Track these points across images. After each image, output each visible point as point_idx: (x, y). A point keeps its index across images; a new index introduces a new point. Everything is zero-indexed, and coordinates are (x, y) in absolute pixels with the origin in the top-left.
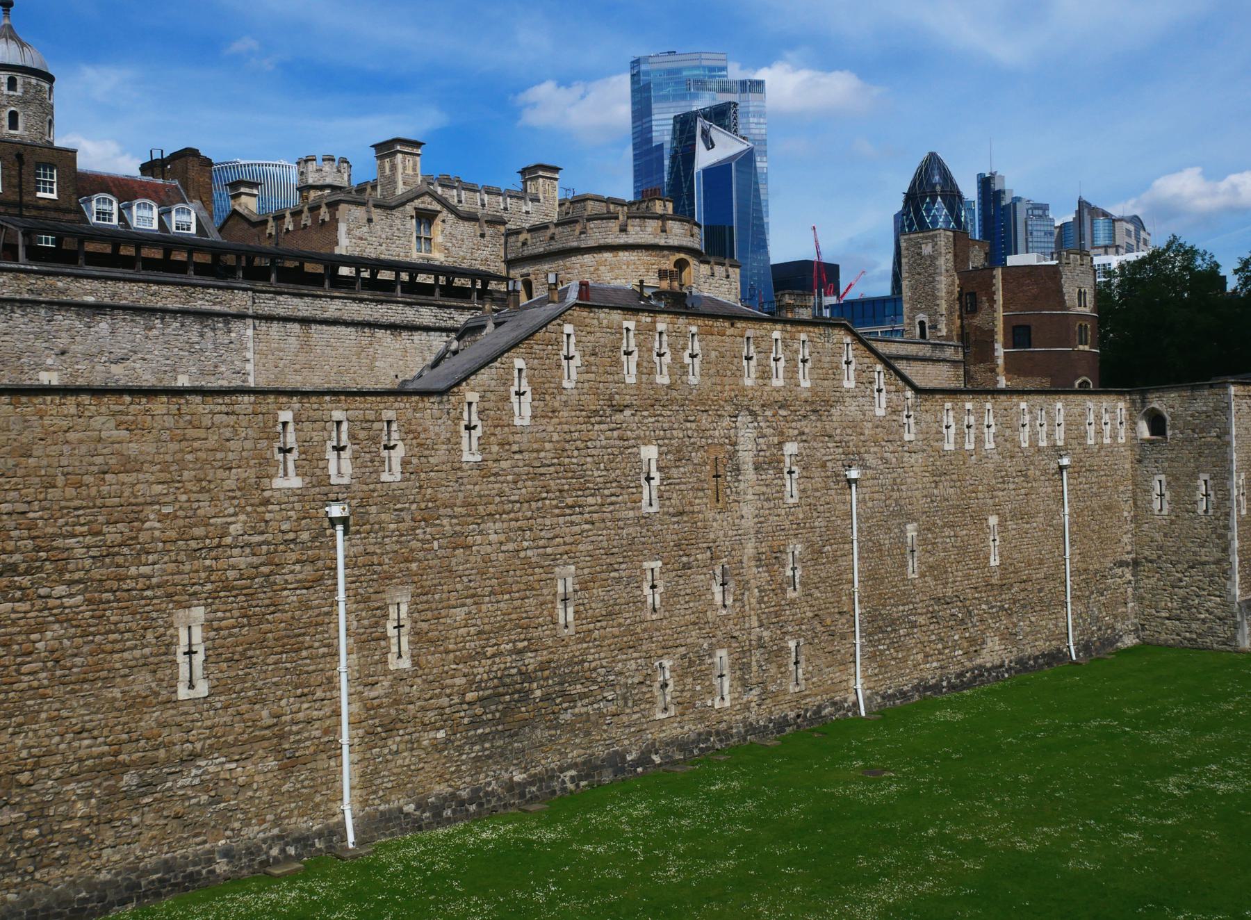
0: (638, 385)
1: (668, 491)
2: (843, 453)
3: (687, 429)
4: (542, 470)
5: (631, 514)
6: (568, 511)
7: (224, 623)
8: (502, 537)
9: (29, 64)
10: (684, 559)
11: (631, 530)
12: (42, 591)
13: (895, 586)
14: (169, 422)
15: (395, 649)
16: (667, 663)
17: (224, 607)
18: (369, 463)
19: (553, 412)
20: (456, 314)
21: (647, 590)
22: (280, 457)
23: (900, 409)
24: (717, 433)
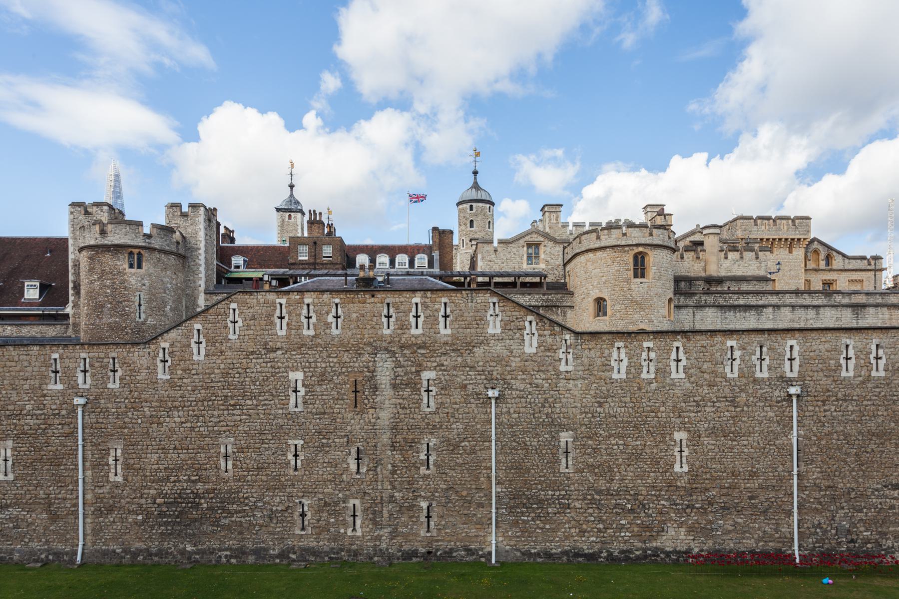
0: (288, 336)
1: (313, 399)
2: (486, 379)
3: (329, 362)
4: (212, 384)
5: (280, 411)
6: (230, 408)
7: (22, 449)
8: (183, 420)
9: (479, 197)
10: (324, 441)
11: (279, 421)
17: (22, 442)
19: (221, 352)
23: (555, 347)
24: (357, 365)
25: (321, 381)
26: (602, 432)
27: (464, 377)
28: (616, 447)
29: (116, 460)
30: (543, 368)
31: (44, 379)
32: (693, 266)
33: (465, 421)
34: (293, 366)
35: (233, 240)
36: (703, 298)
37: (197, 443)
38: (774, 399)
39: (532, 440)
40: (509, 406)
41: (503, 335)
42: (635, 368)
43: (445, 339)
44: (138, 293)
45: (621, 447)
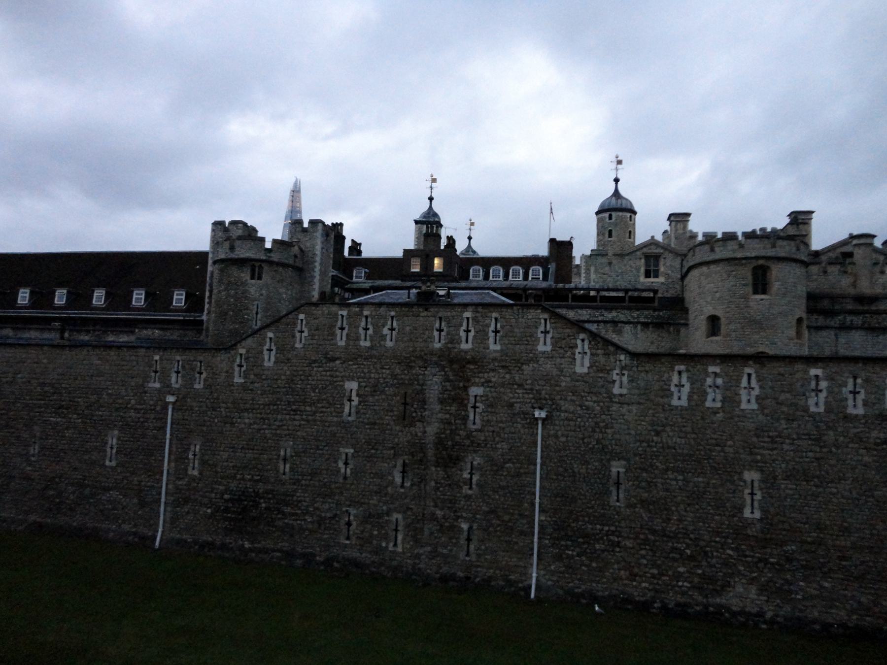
2: (533, 398)
3: (383, 373)
4: (278, 390)
5: (335, 419)
6: (292, 413)
8: (252, 421)
9: (619, 206)
10: (373, 451)
11: (334, 428)
12: (70, 416)
13: (592, 507)
14: (115, 358)
15: (191, 465)
16: (353, 511)
18: (189, 382)
20: (606, 314)
21: (341, 465)
22: (153, 374)
23: (608, 368)
25: (374, 392)
26: (658, 464)
27: (511, 395)
28: (674, 483)
29: (195, 455)
30: (595, 390)
31: (146, 379)
32: (840, 281)
33: (511, 441)
34: (350, 376)
35: (359, 252)
36: (849, 318)
37: (262, 444)
38: (872, 440)
39: (580, 467)
40: (557, 428)
41: (554, 352)
42: (698, 394)
43: (494, 355)
44: (255, 303)
45: (680, 483)
